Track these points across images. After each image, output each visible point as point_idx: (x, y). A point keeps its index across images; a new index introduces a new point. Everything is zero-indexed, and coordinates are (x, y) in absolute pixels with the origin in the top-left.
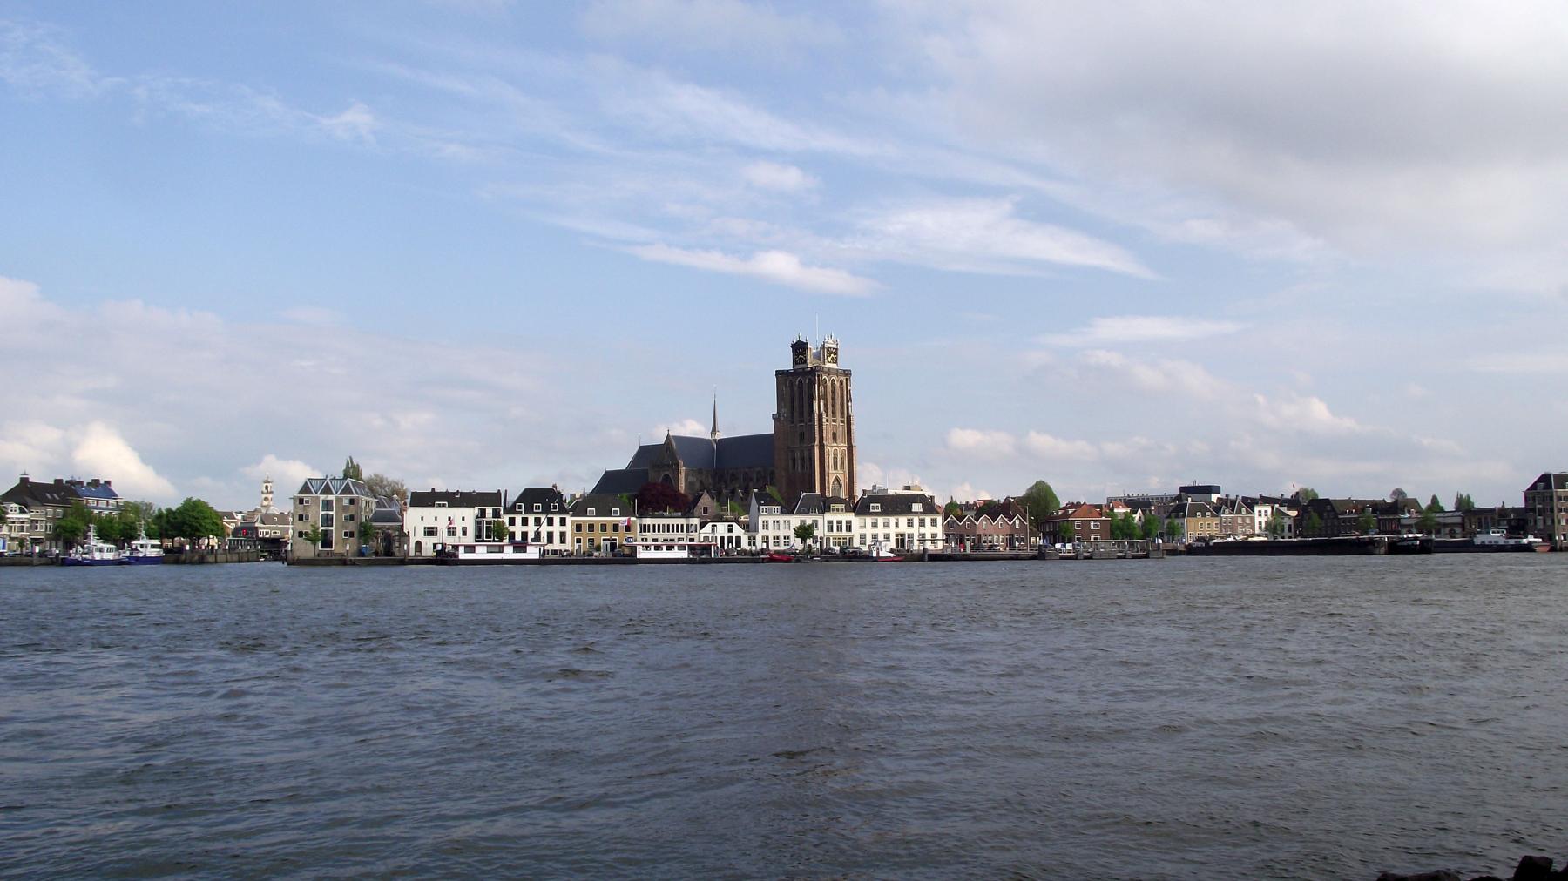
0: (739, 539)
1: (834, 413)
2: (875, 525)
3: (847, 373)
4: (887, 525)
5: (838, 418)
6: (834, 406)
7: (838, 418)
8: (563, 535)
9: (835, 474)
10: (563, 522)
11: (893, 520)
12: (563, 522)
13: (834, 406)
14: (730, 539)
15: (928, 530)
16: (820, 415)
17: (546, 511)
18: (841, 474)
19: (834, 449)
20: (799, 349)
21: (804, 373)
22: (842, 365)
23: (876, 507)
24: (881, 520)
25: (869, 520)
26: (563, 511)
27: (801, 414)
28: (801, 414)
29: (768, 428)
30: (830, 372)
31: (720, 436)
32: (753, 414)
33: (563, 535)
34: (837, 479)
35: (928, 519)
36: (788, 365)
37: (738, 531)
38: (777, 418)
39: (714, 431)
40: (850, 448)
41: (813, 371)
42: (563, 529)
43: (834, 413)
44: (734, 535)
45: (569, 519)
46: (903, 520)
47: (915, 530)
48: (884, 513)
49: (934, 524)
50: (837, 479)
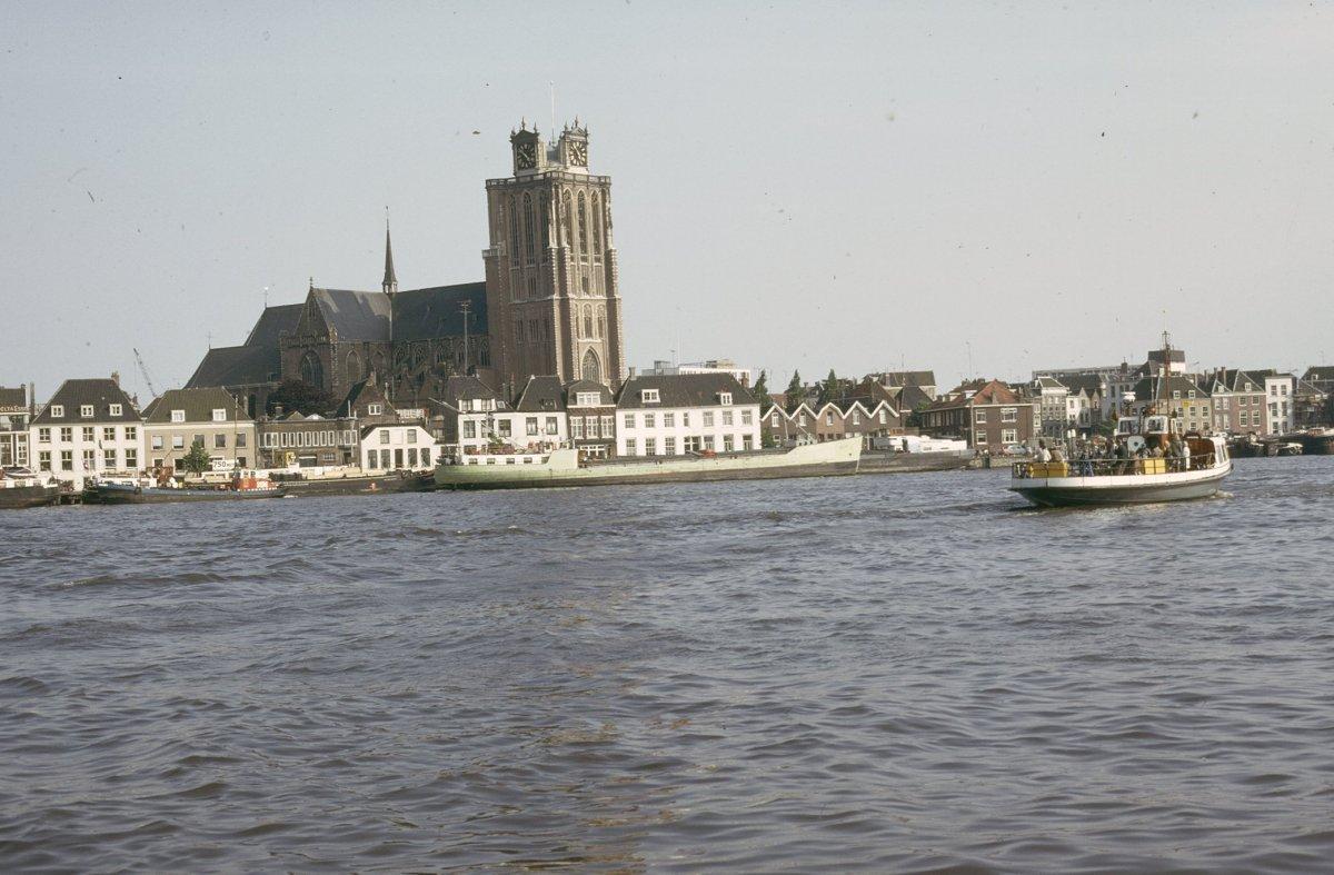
0: (426, 452)
1: (584, 247)
2: (650, 423)
3: (604, 185)
4: (669, 421)
5: (591, 254)
6: (583, 235)
7: (591, 254)
8: (131, 453)
9: (588, 343)
10: (131, 434)
11: (679, 413)
12: (131, 434)
13: (583, 235)
14: (413, 453)
15: (738, 430)
16: (561, 251)
17: (102, 416)
18: (598, 342)
19: (586, 304)
20: (524, 143)
21: (532, 183)
22: (596, 166)
23: (653, 394)
24: (659, 414)
25: (640, 415)
26: (130, 415)
27: (531, 249)
28: (531, 249)
29: (476, 273)
30: (574, 181)
31: (404, 284)
32: (452, 253)
33: (131, 453)
34: (591, 352)
35: (737, 411)
36: (505, 169)
37: (425, 439)
38: (490, 259)
39: (389, 278)
40: (612, 305)
41: (548, 181)
42: (131, 444)
43: (584, 247)
44: (419, 446)
45: (140, 429)
46: (696, 414)
47: (719, 431)
48: (666, 403)
49: (747, 420)
50: (591, 352)
